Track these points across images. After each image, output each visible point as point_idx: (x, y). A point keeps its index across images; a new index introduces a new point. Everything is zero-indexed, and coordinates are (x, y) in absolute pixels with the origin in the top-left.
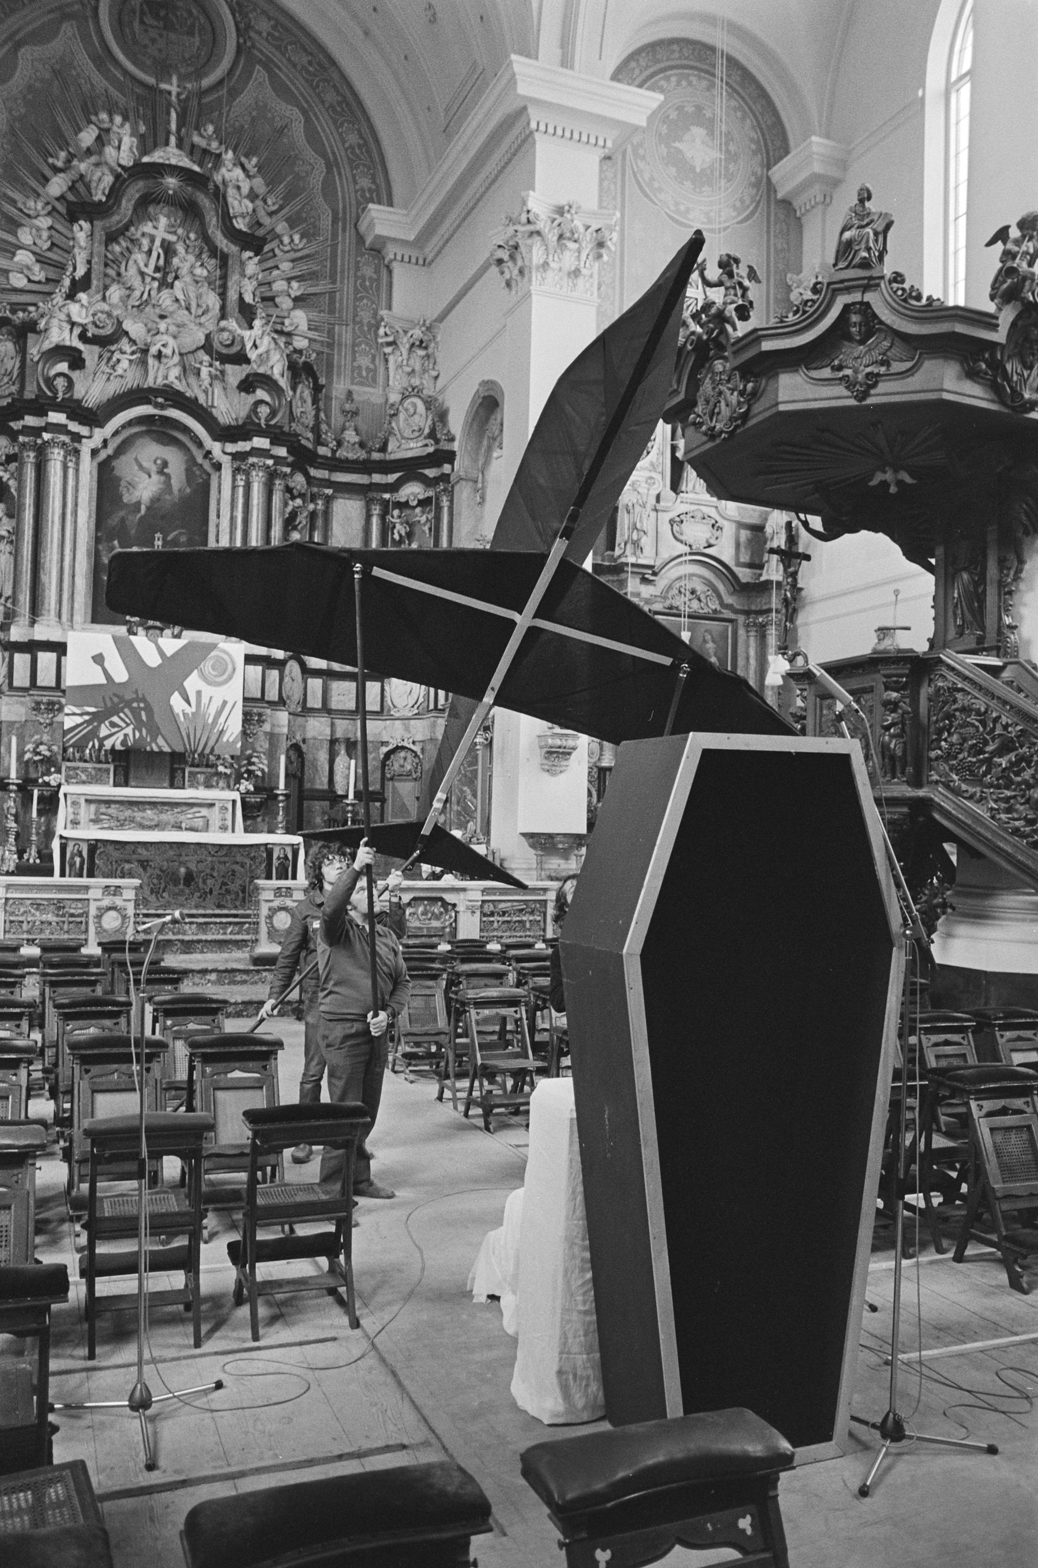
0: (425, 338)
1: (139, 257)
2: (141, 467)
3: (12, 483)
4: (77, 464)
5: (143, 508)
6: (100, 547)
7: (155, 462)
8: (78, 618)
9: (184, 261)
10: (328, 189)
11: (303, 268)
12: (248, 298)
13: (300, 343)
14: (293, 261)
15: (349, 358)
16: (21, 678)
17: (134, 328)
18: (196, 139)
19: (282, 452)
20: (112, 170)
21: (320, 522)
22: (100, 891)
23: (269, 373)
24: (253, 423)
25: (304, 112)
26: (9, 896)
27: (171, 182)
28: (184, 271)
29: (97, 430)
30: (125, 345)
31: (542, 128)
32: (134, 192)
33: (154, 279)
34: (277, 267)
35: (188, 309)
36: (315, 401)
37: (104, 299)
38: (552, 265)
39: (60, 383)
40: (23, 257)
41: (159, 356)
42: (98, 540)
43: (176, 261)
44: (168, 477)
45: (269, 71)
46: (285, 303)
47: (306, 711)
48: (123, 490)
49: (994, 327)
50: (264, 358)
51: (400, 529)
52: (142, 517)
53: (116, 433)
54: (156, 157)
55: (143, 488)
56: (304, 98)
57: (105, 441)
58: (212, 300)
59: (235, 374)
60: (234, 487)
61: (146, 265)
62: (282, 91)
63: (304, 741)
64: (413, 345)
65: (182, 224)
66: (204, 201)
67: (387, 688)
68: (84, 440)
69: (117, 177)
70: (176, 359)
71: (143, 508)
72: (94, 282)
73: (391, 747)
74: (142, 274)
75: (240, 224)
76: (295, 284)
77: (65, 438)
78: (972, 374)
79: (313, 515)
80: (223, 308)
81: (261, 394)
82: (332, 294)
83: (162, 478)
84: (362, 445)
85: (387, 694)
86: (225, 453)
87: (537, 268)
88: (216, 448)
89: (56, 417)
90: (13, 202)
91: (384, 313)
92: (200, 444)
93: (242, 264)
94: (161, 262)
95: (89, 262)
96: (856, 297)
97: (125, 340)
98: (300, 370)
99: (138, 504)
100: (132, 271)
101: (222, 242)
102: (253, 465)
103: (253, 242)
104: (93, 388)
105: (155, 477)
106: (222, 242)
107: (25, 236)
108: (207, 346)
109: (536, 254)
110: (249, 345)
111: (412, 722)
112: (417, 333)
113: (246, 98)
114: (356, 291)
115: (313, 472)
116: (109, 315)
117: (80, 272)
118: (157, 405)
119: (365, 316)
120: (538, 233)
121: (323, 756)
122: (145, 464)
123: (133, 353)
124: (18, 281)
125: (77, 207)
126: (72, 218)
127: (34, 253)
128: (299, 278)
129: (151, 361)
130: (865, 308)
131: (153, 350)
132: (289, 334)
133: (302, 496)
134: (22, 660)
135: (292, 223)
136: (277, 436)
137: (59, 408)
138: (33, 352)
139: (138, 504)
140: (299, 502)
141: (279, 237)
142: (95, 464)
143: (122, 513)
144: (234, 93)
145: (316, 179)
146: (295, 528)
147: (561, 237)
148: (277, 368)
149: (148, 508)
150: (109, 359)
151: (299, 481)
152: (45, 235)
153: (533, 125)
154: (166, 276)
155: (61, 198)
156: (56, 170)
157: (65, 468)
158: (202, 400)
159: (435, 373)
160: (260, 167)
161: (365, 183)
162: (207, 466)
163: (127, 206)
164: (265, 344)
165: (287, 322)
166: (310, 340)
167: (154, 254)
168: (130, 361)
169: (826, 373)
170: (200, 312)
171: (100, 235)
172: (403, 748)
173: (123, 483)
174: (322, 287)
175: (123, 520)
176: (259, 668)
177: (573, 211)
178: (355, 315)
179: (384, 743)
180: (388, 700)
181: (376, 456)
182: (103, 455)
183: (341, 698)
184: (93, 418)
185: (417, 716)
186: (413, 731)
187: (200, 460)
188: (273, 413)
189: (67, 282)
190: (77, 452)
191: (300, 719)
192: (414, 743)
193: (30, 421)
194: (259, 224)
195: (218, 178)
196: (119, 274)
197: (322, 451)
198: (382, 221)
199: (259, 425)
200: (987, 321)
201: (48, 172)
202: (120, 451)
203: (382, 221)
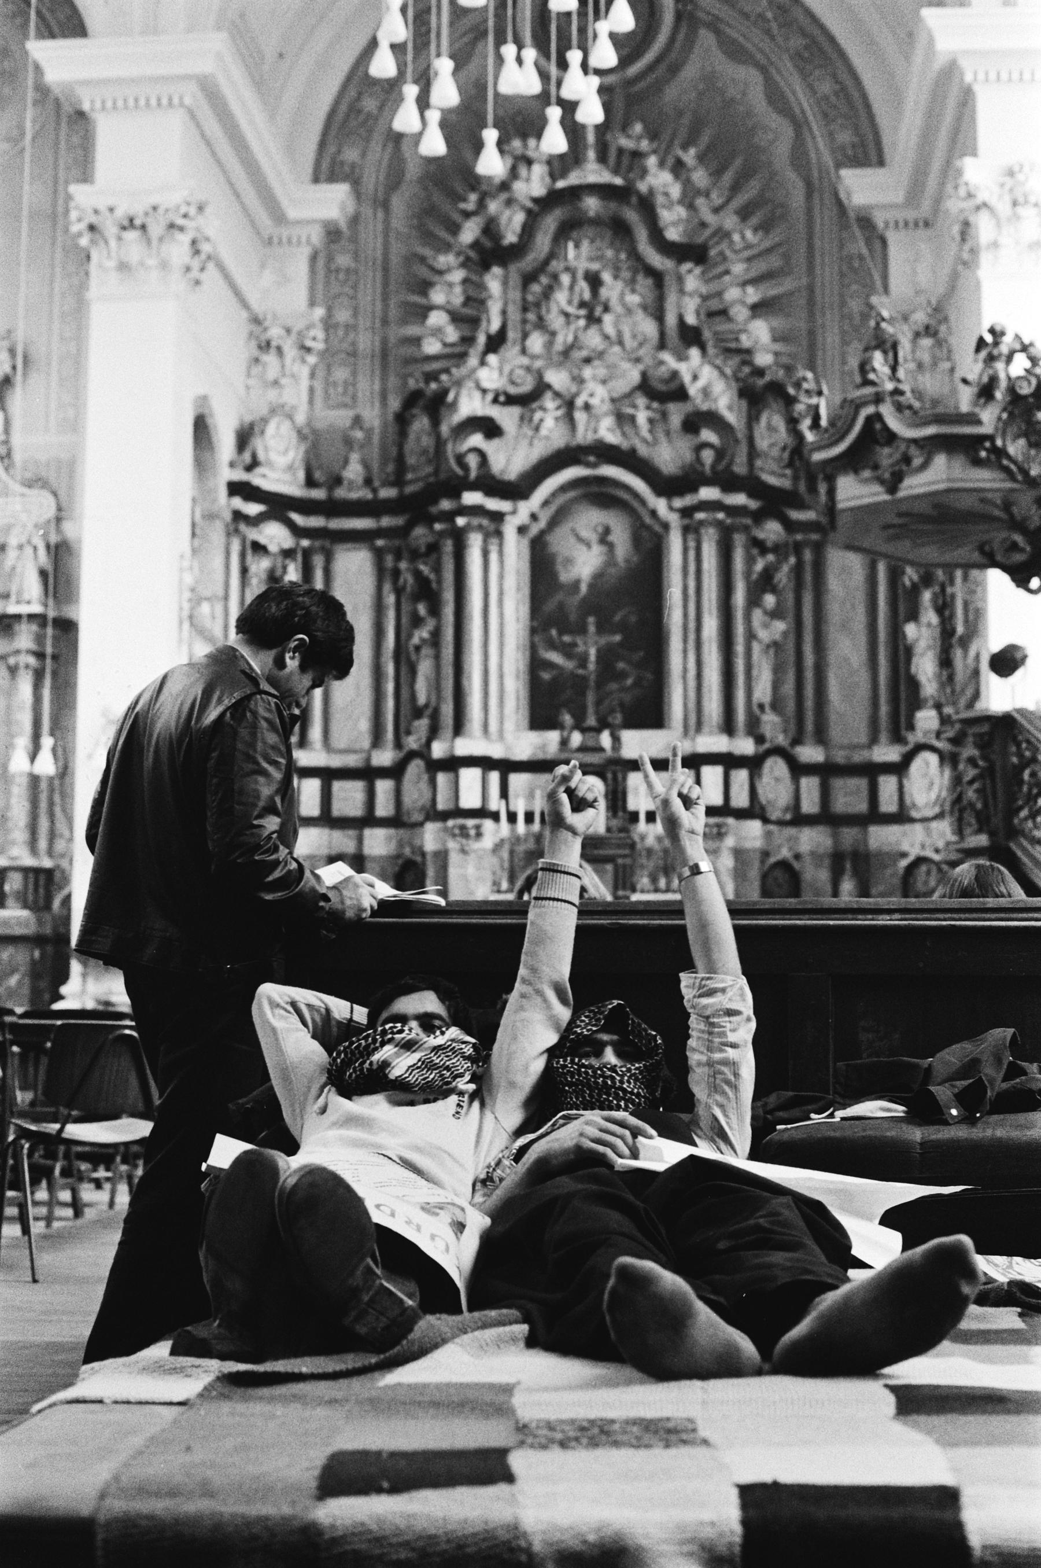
0: (933, 322)
1: (561, 297)
2: (580, 539)
3: (432, 576)
4: (501, 545)
6: (536, 639)
7: (595, 530)
8: (509, 725)
9: (612, 289)
10: (799, 157)
11: (761, 267)
12: (691, 319)
13: (763, 359)
14: (749, 260)
15: (837, 361)
17: (558, 378)
18: (624, 142)
19: (740, 499)
20: (523, 208)
21: (808, 577)
23: (713, 407)
24: (695, 471)
25: (763, 70)
27: (592, 204)
28: (614, 302)
30: (549, 402)
31: (981, 76)
32: (550, 223)
33: (578, 317)
34: (727, 272)
35: (621, 343)
37: (524, 351)
38: (1003, 240)
39: (473, 461)
40: (437, 318)
41: (587, 407)
42: (533, 631)
43: (604, 292)
44: (611, 547)
45: (718, 32)
46: (740, 313)
47: (799, 819)
48: (559, 567)
49: (979, 422)
50: (706, 392)
51: (911, 575)
52: (584, 600)
53: (546, 503)
54: (574, 178)
55: (583, 564)
56: (762, 51)
57: (534, 517)
58: (649, 327)
59: (676, 414)
60: (685, 550)
61: (570, 302)
62: (736, 52)
63: (797, 857)
64: (917, 335)
65: (612, 244)
66: (632, 216)
67: (905, 781)
68: (508, 518)
69: (529, 212)
70: (607, 407)
71: (584, 588)
72: (512, 334)
74: (567, 315)
75: (673, 234)
76: (750, 290)
77: (485, 522)
78: (977, 462)
79: (798, 570)
80: (662, 334)
81: (708, 435)
82: (811, 289)
83: (604, 549)
86: (671, 508)
87: (988, 247)
88: (661, 505)
89: (471, 498)
90: (423, 260)
91: (874, 300)
92: (643, 502)
93: (680, 280)
94: (587, 295)
95: (504, 313)
96: (870, 410)
97: (548, 395)
98: (759, 392)
99: (577, 583)
100: (554, 309)
101: (656, 259)
102: (701, 523)
103: (692, 253)
104: (509, 458)
106: (656, 259)
107: (438, 296)
108: (645, 387)
109: (984, 228)
110: (687, 379)
111: (934, 825)
112: (920, 317)
113: (690, 72)
114: (842, 275)
115: (795, 515)
116: (528, 369)
117: (495, 326)
118: (588, 465)
119: (855, 305)
120: (985, 204)
121: (824, 875)
122: (585, 534)
123: (558, 408)
124: (432, 347)
125: (490, 253)
126: (486, 266)
127: (449, 312)
128: (754, 281)
129: (580, 416)
130: (878, 417)
131: (579, 402)
132: (748, 352)
133: (776, 549)
135: (744, 214)
136: (729, 483)
137: (473, 487)
138: (445, 429)
139: (577, 583)
140: (771, 557)
141: (727, 235)
142: (525, 543)
143: (559, 596)
144: (674, 70)
145: (782, 149)
146: (774, 590)
147: (1015, 204)
148: (724, 401)
149: (591, 586)
150: (531, 420)
151: (772, 530)
152: (458, 290)
153: (968, 78)
154: (592, 312)
155: (476, 245)
156: (467, 215)
157: (485, 554)
158: (643, 450)
159: (947, 365)
160: (701, 158)
161: (845, 137)
162: (657, 528)
163: (543, 242)
164: (707, 374)
165: (743, 337)
166: (776, 354)
167: (577, 289)
168: (557, 419)
169: (867, 474)
170: (635, 344)
171: (515, 279)
173: (559, 560)
174: (787, 285)
175: (561, 606)
177: (1026, 169)
178: (843, 304)
180: (908, 801)
182: (535, 530)
183: (848, 799)
184: (516, 490)
187: (648, 520)
188: (720, 454)
189: (482, 339)
190: (499, 534)
191: (791, 831)
192: (937, 851)
193: (446, 505)
194: (703, 225)
195: (642, 187)
196: (541, 318)
198: (861, 188)
199: (702, 473)
200: (973, 419)
201: (456, 217)
202: (554, 522)
203: (861, 188)
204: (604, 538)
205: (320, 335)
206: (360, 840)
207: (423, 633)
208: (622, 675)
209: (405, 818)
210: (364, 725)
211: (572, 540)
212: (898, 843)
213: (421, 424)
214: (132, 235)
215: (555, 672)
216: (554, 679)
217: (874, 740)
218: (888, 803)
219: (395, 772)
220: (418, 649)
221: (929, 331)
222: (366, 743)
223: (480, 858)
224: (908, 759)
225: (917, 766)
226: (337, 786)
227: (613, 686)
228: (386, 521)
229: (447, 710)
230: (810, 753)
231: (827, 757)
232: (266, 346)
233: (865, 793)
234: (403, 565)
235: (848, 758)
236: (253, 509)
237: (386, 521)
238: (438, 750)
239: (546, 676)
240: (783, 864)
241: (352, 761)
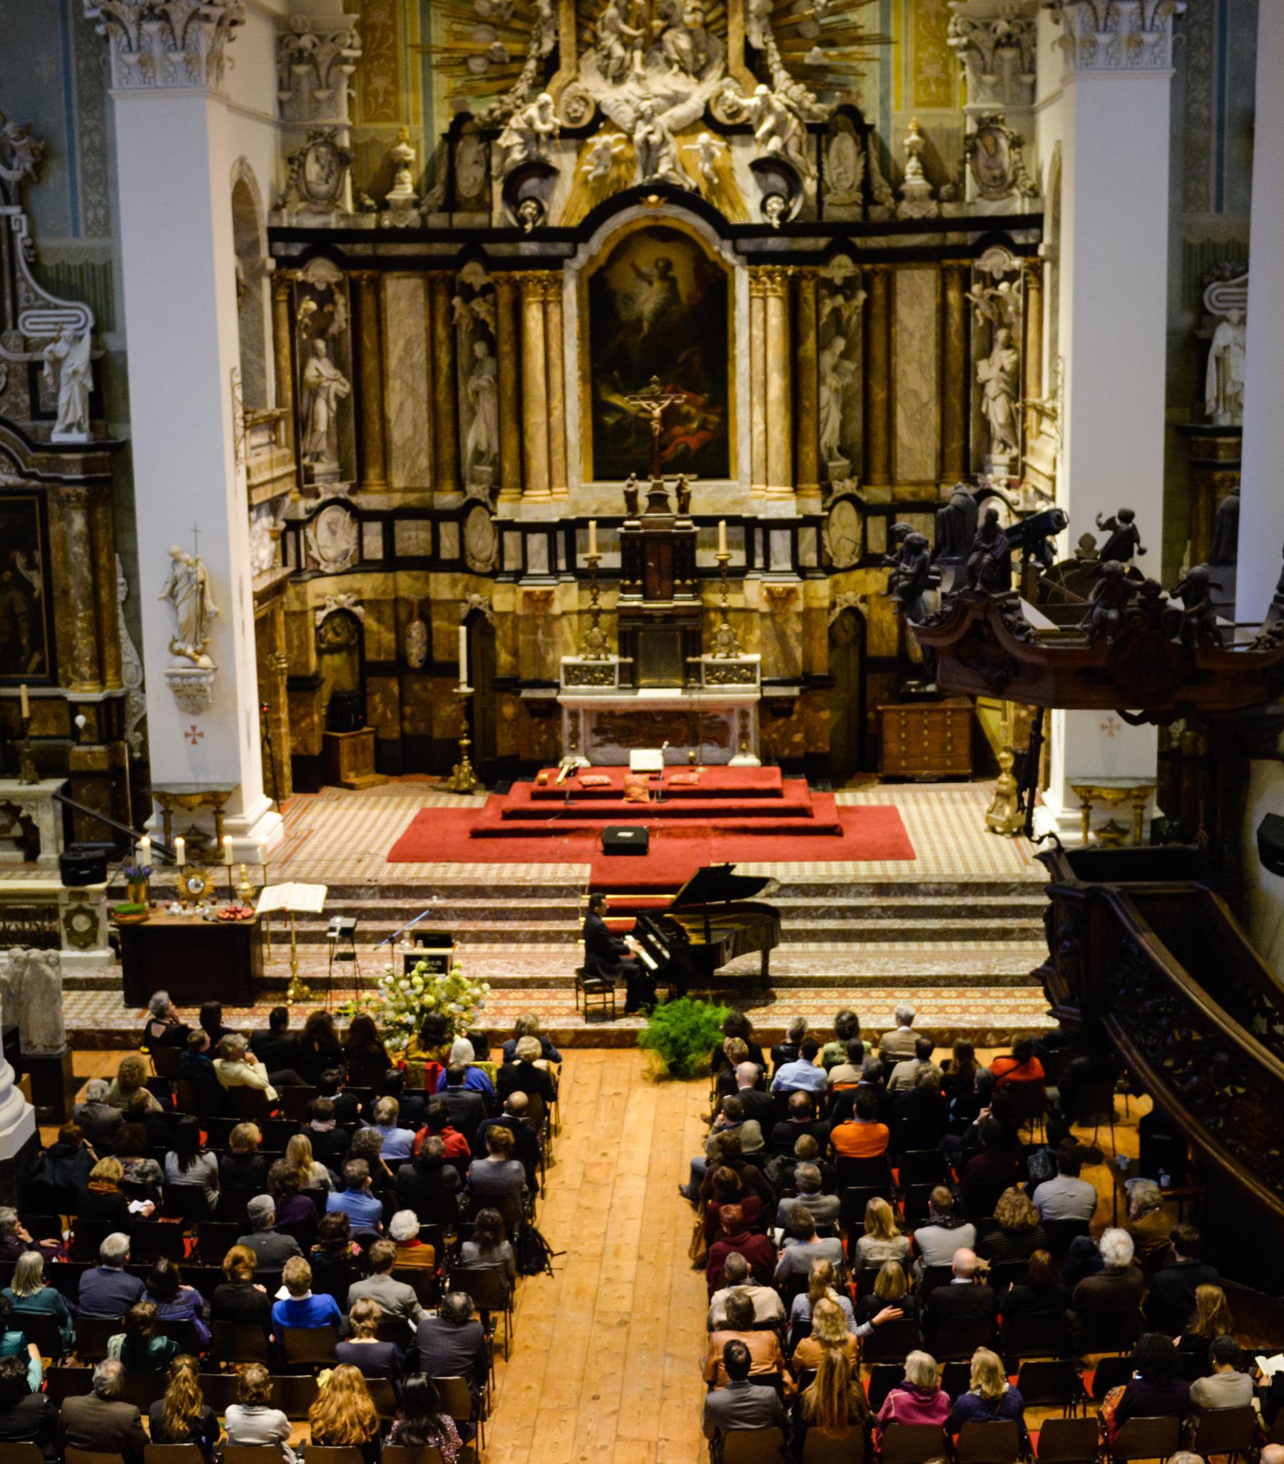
2: (641, 275)
3: (488, 319)
5: (646, 325)
8: (573, 479)
29: (581, 247)
36: (863, 147)
44: (673, 282)
68: (567, 261)
71: (646, 325)
72: (564, 61)
79: (867, 304)
83: (667, 285)
84: (934, 195)
99: (640, 320)
105: (657, 285)
112: (1003, 26)
122: (645, 269)
130: (989, 625)
143: (620, 337)
149: (652, 325)
173: (619, 297)
181: (950, 210)
189: (532, 65)
191: (859, 574)
197: (877, 213)
204: (665, 270)
205: (357, 41)
206: (427, 582)
207: (484, 380)
208: (688, 418)
209: (470, 563)
210: (424, 462)
211: (632, 275)
213: (469, 151)
214: (152, 27)
215: (618, 416)
216: (618, 423)
217: (941, 477)
219: (460, 515)
220: (476, 393)
221: (1008, 41)
222: (427, 484)
226: (400, 525)
227: (678, 430)
228: (438, 249)
229: (509, 466)
230: (878, 493)
231: (893, 495)
232: (300, 56)
234: (457, 301)
235: (914, 494)
236: (296, 250)
237: (438, 249)
238: (504, 510)
239: (610, 420)
240: (852, 611)
241: (412, 498)
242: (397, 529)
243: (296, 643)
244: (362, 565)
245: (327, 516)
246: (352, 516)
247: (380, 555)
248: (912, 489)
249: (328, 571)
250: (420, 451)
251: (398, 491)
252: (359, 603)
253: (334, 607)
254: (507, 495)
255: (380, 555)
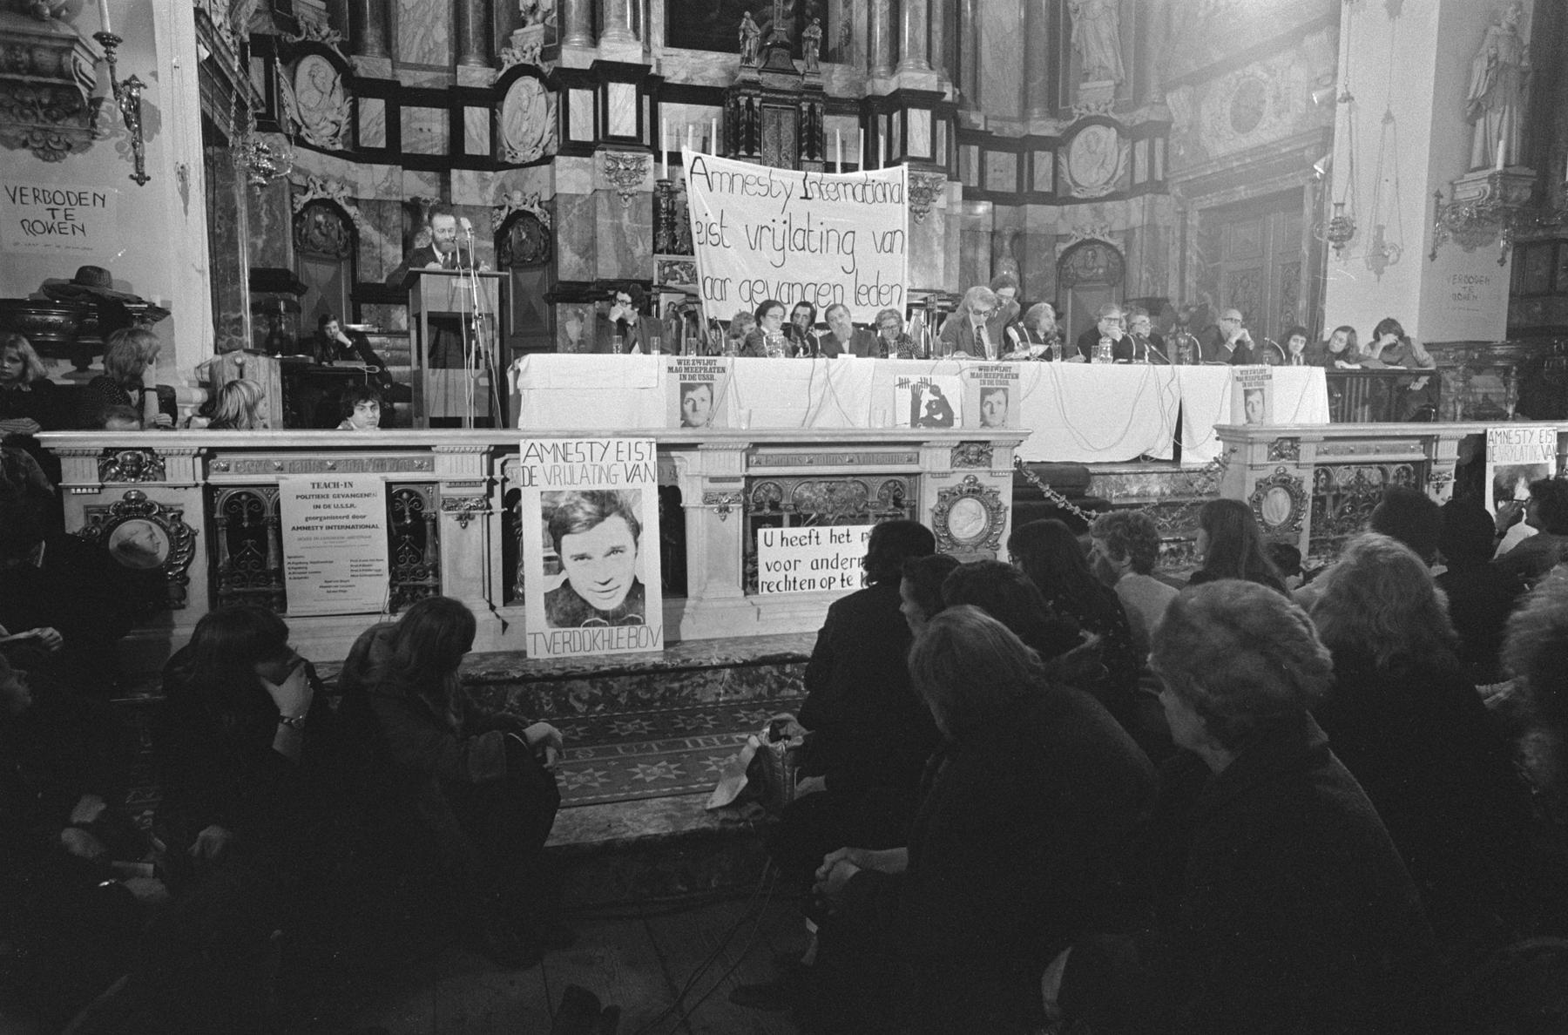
16: (581, 129)
22: (947, 454)
26: (753, 471)
67: (1063, 160)
73: (1072, 242)
85: (1064, 168)
111: (1109, 205)
134: (580, 100)
172: (1093, 242)
176: (927, 114)
179: (1060, 238)
185: (1110, 197)
186: (1109, 218)
192: (1111, 234)
206: (445, 184)
210: (442, 34)
212: (1055, 223)
218: (1043, 184)
219: (492, 97)
223: (639, 205)
224: (1072, 133)
225: (1078, 143)
226: (405, 111)
233: (1013, 172)
235: (1001, 129)
241: (424, 79)
242: (403, 118)
243: (265, 221)
244: (358, 153)
245: (307, 64)
246: (345, 83)
247: (382, 144)
248: (999, 124)
249: (311, 141)
250: (436, 18)
251: (407, 66)
252: (354, 201)
253: (320, 194)
254: (577, 38)
255: (382, 144)
